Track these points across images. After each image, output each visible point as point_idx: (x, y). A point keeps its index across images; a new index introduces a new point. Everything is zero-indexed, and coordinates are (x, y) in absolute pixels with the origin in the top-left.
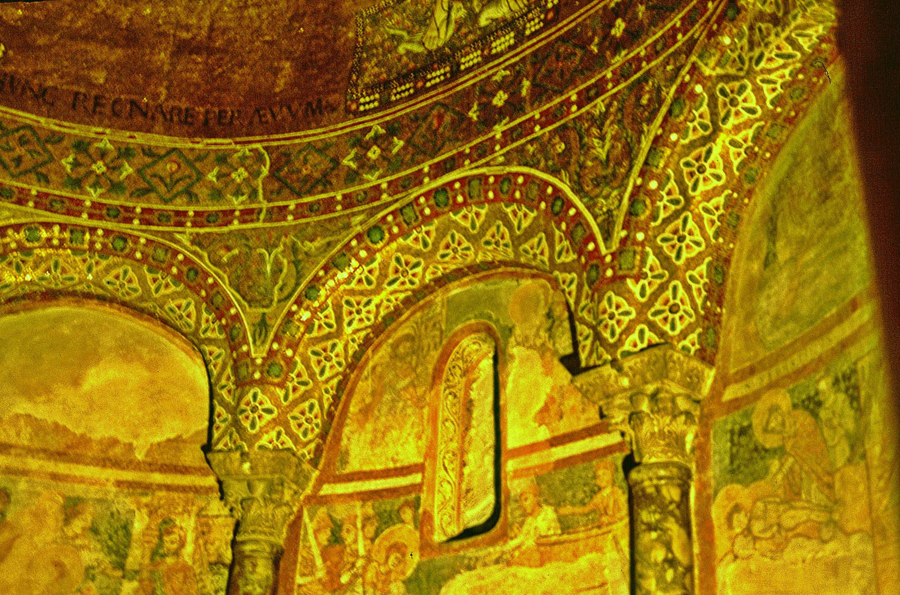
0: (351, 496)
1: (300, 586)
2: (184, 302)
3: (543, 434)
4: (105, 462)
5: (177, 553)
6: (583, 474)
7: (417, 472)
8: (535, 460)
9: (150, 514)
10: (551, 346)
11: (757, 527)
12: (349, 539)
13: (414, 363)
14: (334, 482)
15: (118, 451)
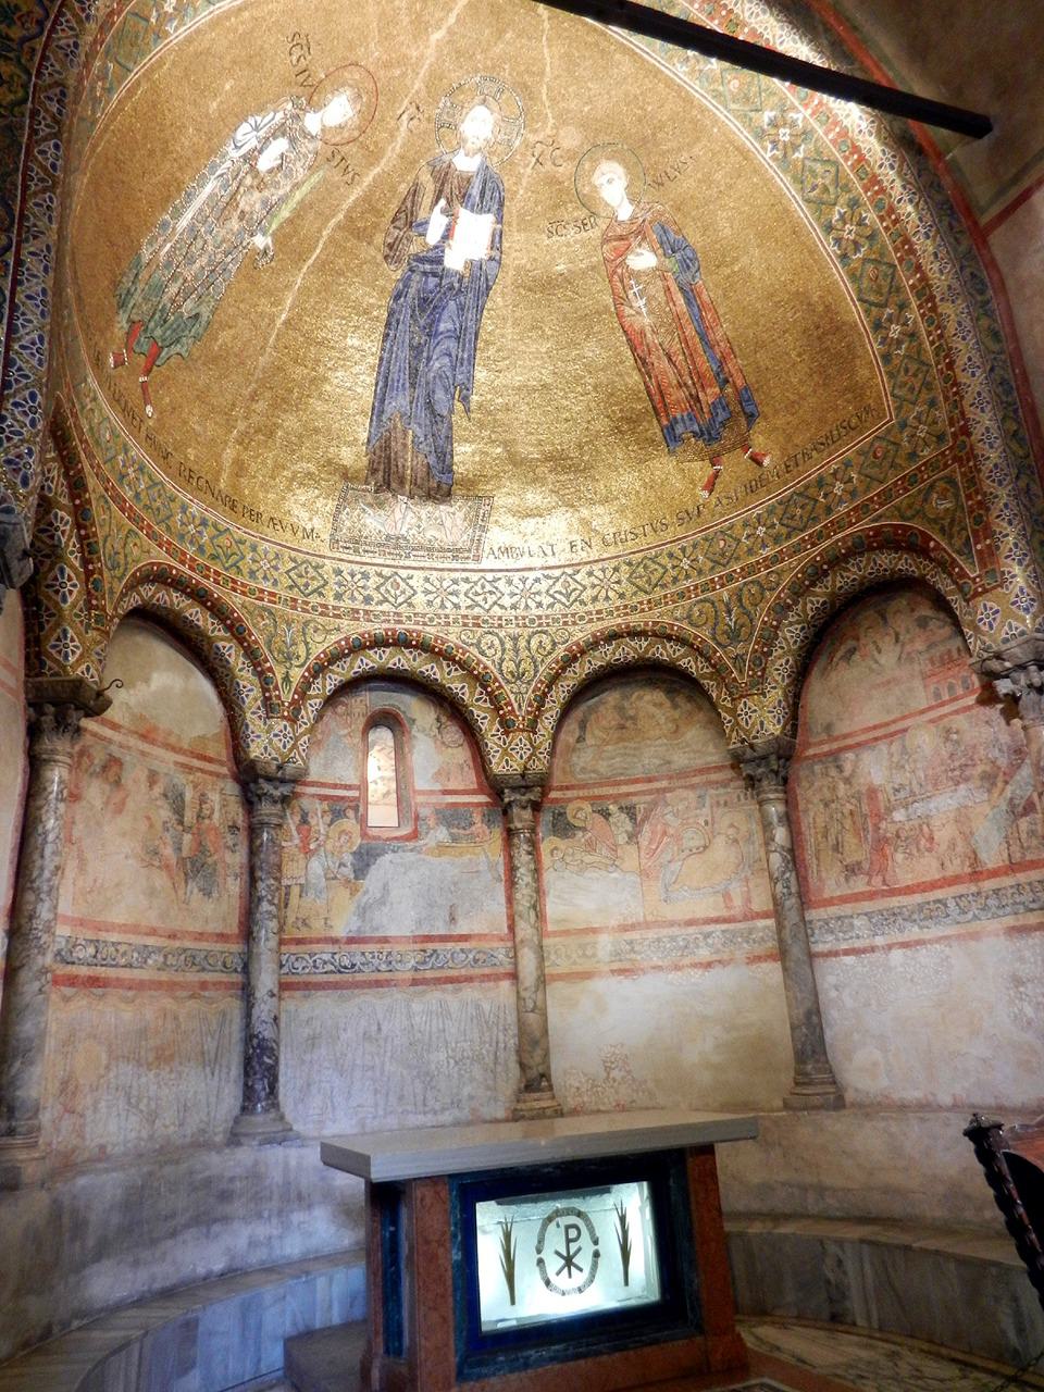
0: (313, 796)
2: (228, 645)
3: (438, 787)
8: (433, 799)
9: (195, 787)
11: (568, 859)
12: (313, 822)
15: (172, 740)
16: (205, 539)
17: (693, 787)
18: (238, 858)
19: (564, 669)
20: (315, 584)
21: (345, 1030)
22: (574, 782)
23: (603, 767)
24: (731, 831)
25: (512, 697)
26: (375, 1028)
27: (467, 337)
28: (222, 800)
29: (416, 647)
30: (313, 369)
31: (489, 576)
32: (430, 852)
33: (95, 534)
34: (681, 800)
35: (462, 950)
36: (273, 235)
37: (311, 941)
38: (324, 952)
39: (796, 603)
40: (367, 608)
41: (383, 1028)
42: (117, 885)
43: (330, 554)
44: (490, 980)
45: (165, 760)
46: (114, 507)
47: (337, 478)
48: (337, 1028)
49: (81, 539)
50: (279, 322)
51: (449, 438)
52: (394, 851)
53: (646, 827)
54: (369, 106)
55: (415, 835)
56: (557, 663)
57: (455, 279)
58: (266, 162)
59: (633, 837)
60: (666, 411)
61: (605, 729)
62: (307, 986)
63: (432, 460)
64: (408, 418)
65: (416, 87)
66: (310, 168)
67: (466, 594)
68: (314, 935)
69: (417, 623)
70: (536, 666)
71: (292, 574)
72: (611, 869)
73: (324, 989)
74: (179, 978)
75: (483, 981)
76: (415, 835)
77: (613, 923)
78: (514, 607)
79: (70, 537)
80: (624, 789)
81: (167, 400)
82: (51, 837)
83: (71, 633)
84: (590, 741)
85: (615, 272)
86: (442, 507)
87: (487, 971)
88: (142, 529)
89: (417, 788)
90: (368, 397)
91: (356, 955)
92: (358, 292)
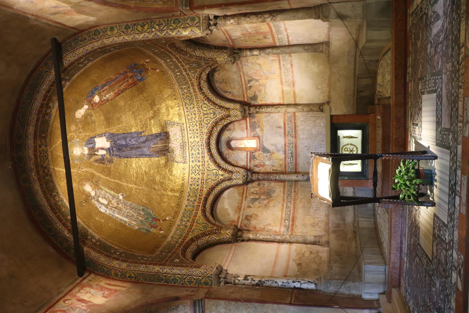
0: (250, 164)
3: (246, 131)
4: (241, 203)
5: (257, 191)
8: (249, 132)
9: (250, 195)
11: (263, 97)
12: (256, 164)
15: (240, 202)
16: (192, 199)
17: (242, 67)
18: (266, 184)
19: (211, 101)
20: (197, 168)
22: (242, 95)
23: (237, 87)
24: (255, 59)
25: (220, 115)
26: (306, 148)
27: (125, 136)
28: (253, 188)
29: (209, 140)
30: (144, 175)
31: (187, 121)
32: (263, 133)
33: (201, 234)
34: (246, 69)
35: (288, 125)
36: (118, 194)
37: (285, 164)
38: (288, 160)
39: (189, 53)
40: (201, 153)
42: (273, 215)
43: (188, 164)
45: (245, 204)
46: (193, 228)
47: (168, 163)
49: (202, 237)
50: (136, 187)
51: (152, 135)
53: (254, 77)
54: (84, 181)
55: (259, 137)
56: (209, 103)
57: (112, 143)
58: (106, 202)
59: (257, 81)
60: (135, 82)
61: (227, 87)
62: (296, 165)
63: (158, 139)
64: (149, 147)
65: (76, 171)
66: (101, 190)
67: (193, 127)
68: (284, 163)
69: (203, 140)
70: (211, 109)
71: (196, 174)
72: (266, 86)
74: (293, 198)
76: (259, 137)
77: (281, 86)
78: (195, 114)
79: (203, 239)
80: (243, 82)
81: (163, 213)
82: (264, 237)
83: (222, 237)
84: (230, 90)
85: (101, 104)
86: (170, 134)
87: (293, 119)
88: (195, 219)
90: (147, 159)
91: (289, 152)
92: (122, 167)
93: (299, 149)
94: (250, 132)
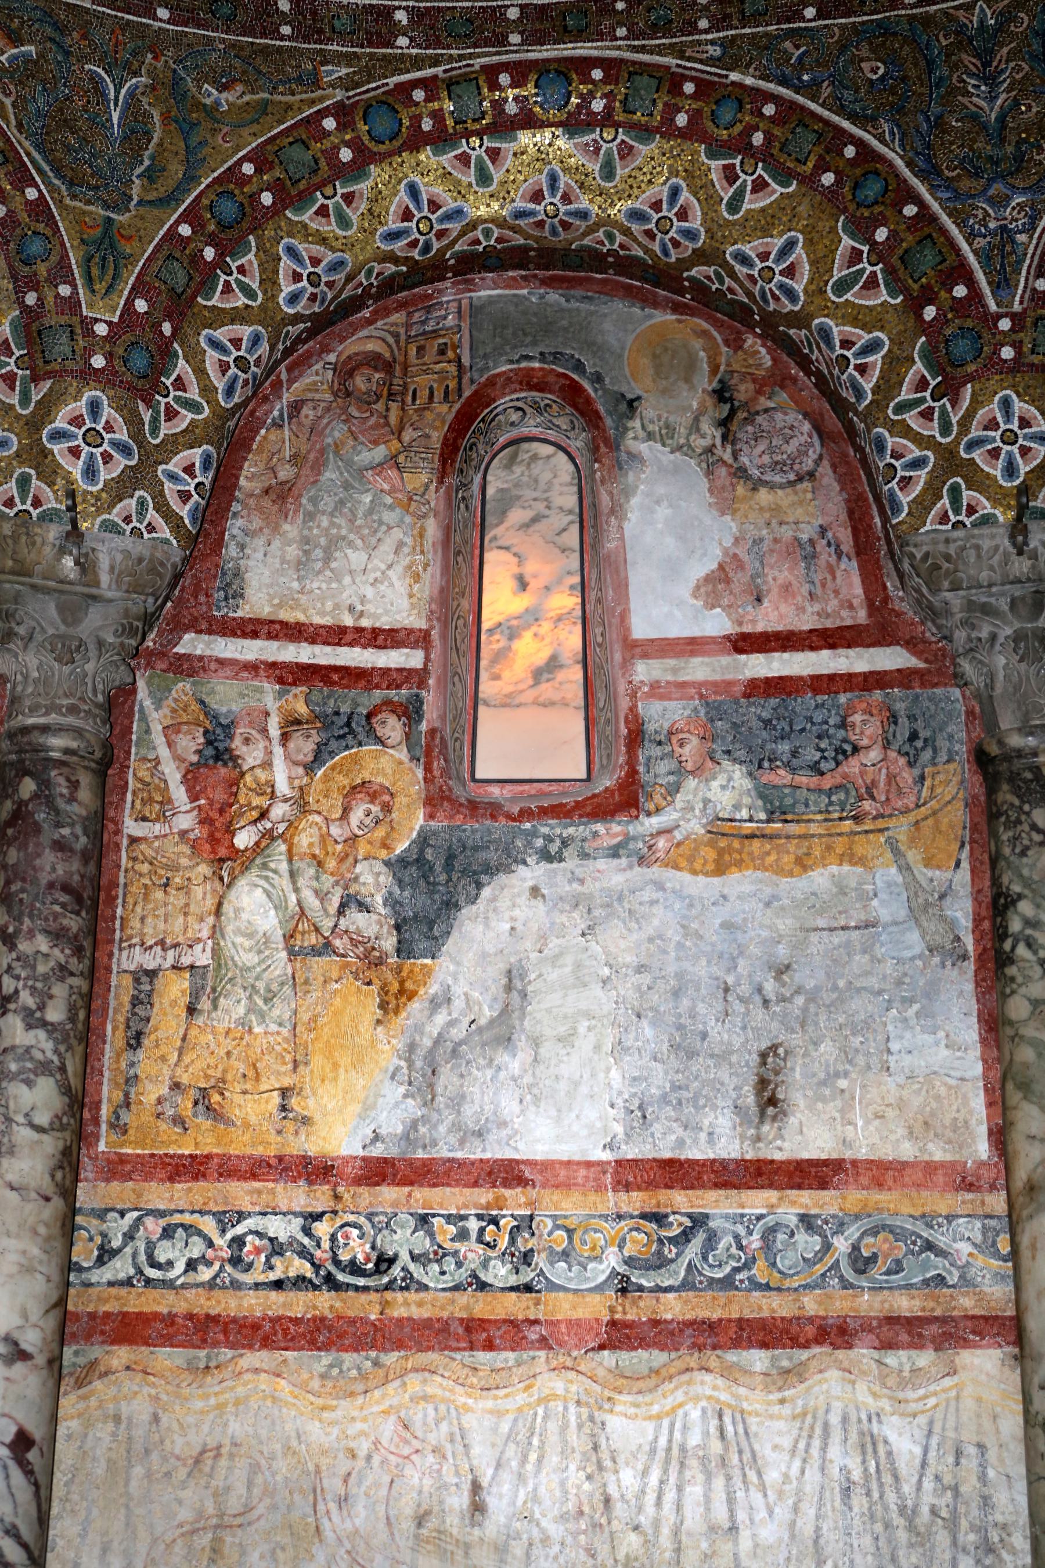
0: (252, 668)
1: (134, 840)
6: (818, 718)
7: (414, 646)
10: (727, 456)
12: (251, 756)
13: (393, 419)
14: (210, 632)
21: (343, 1501)
26: (459, 1501)
41: (492, 1502)
44: (916, 1344)
48: (316, 1493)
52: (547, 856)
73: (267, 1343)
75: (888, 1345)
87: (905, 1305)
89: (641, 629)
93: (436, 1385)
94: (702, 690)
